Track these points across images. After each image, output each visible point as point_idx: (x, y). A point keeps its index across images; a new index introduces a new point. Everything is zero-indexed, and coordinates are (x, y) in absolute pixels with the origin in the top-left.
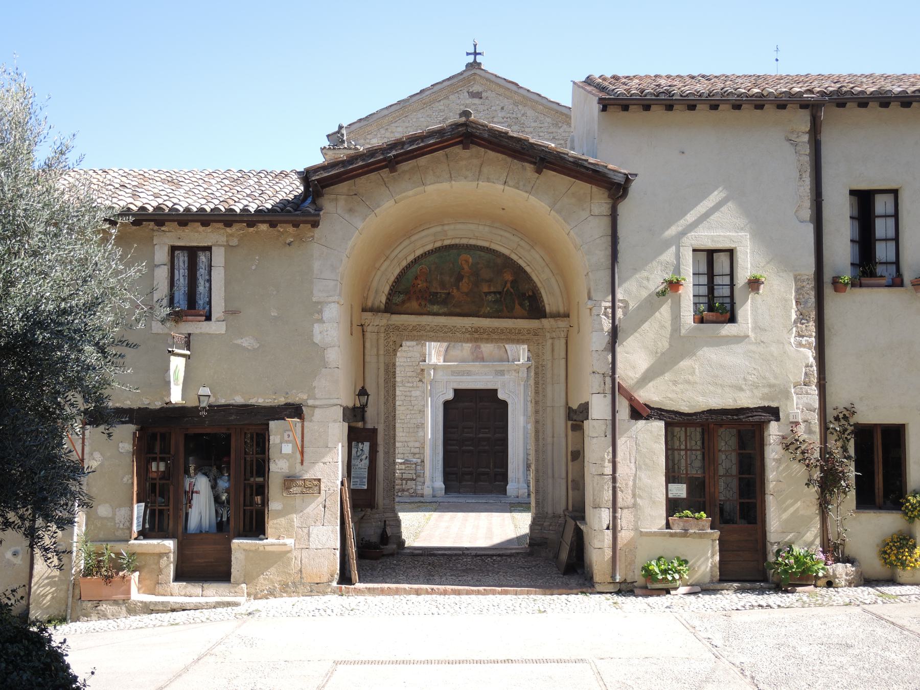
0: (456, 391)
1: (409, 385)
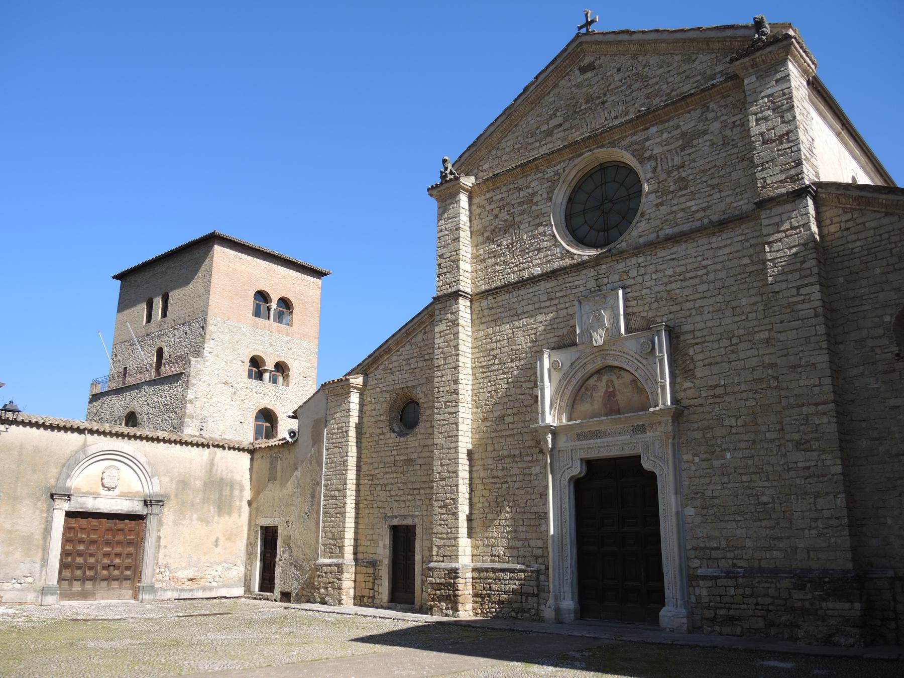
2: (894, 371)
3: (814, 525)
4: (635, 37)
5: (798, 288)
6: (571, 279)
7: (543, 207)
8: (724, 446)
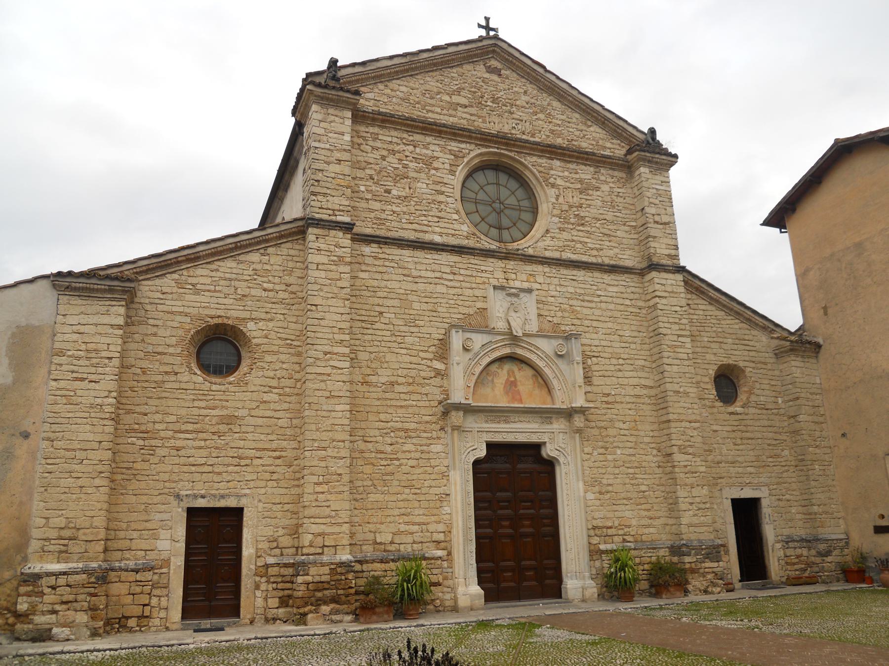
0: (490, 446)
1: (425, 435)
2: (714, 407)
3: (691, 507)
4: (548, 75)
5: (679, 336)
6: (476, 262)
7: (448, 178)
8: (615, 444)
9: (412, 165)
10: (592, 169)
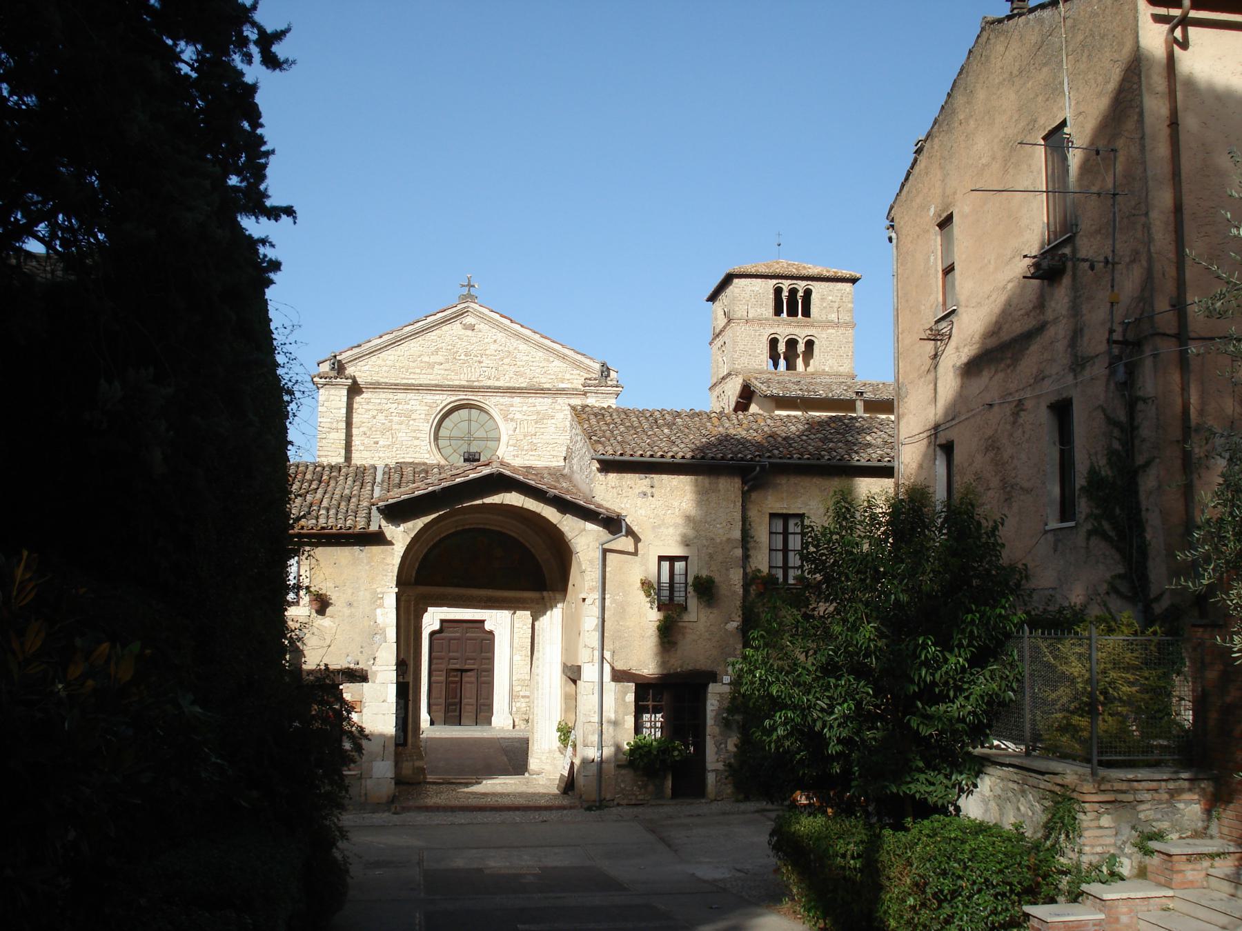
0: (442, 621)
9: (396, 419)
10: (550, 400)
